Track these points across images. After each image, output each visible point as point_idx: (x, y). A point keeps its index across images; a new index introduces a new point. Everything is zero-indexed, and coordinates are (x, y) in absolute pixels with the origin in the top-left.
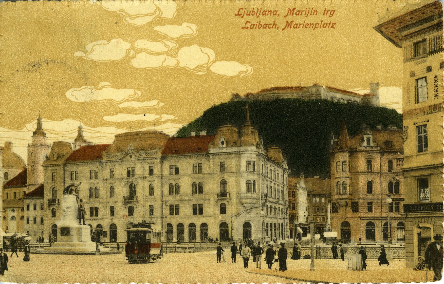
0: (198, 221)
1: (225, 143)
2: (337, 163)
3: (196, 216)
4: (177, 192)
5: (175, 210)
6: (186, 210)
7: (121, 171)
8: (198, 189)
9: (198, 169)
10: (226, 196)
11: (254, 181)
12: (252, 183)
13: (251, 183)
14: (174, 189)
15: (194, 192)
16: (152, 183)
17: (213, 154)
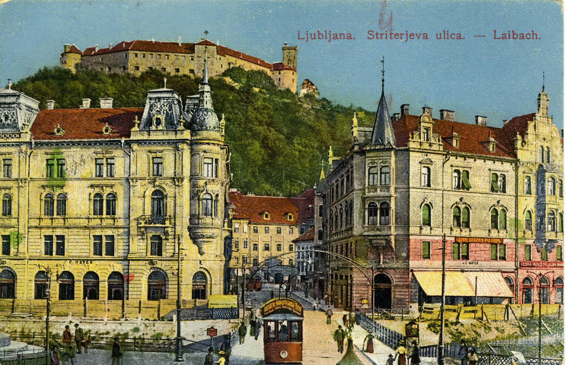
1: (163, 121)
2: (369, 170)
3: (98, 257)
4: (62, 211)
5: (56, 246)
6: (79, 245)
8: (104, 205)
10: (165, 224)
11: (217, 195)
13: (212, 199)
14: (56, 206)
15: (98, 212)
17: (139, 142)
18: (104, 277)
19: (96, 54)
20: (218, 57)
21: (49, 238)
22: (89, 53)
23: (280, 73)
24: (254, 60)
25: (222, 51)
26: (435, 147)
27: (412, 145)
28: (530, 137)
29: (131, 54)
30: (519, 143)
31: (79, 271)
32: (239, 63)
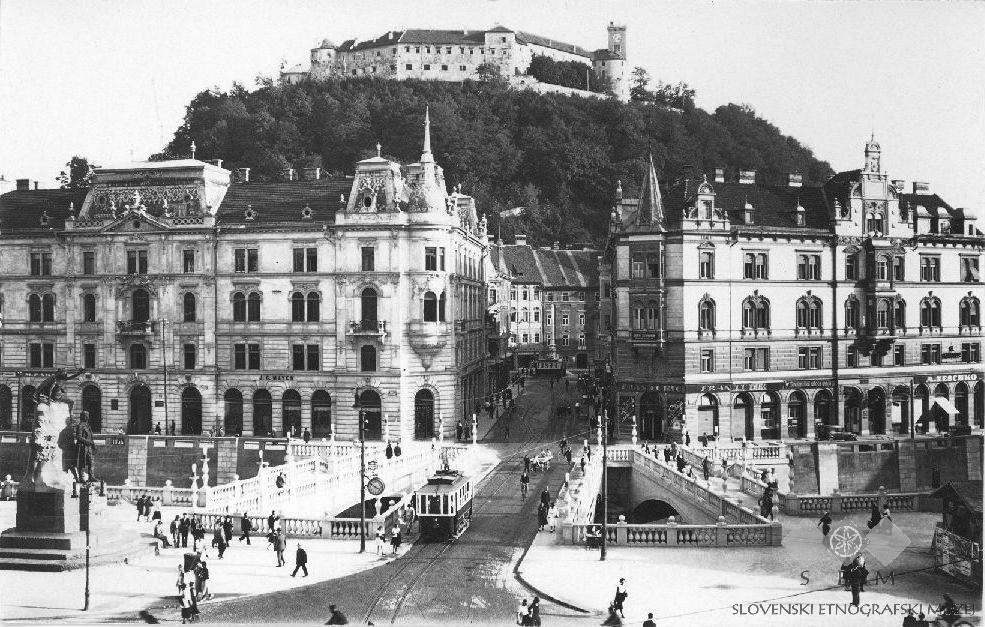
0: (306, 385)
7: (114, 258)
8: (306, 306)
9: (306, 261)
12: (438, 298)
16: (192, 290)
17: (346, 228)
18: (306, 392)
19: (355, 49)
20: (519, 46)
21: (239, 348)
22: (347, 47)
23: (604, 64)
24: (570, 49)
25: (522, 40)
26: (718, 226)
27: (687, 225)
28: (856, 204)
29: (401, 48)
30: (838, 211)
31: (278, 389)
32: (548, 52)
